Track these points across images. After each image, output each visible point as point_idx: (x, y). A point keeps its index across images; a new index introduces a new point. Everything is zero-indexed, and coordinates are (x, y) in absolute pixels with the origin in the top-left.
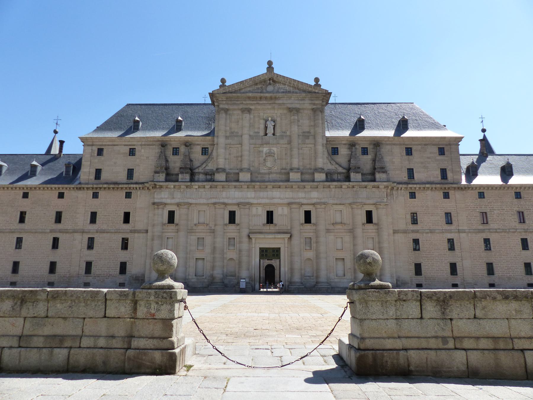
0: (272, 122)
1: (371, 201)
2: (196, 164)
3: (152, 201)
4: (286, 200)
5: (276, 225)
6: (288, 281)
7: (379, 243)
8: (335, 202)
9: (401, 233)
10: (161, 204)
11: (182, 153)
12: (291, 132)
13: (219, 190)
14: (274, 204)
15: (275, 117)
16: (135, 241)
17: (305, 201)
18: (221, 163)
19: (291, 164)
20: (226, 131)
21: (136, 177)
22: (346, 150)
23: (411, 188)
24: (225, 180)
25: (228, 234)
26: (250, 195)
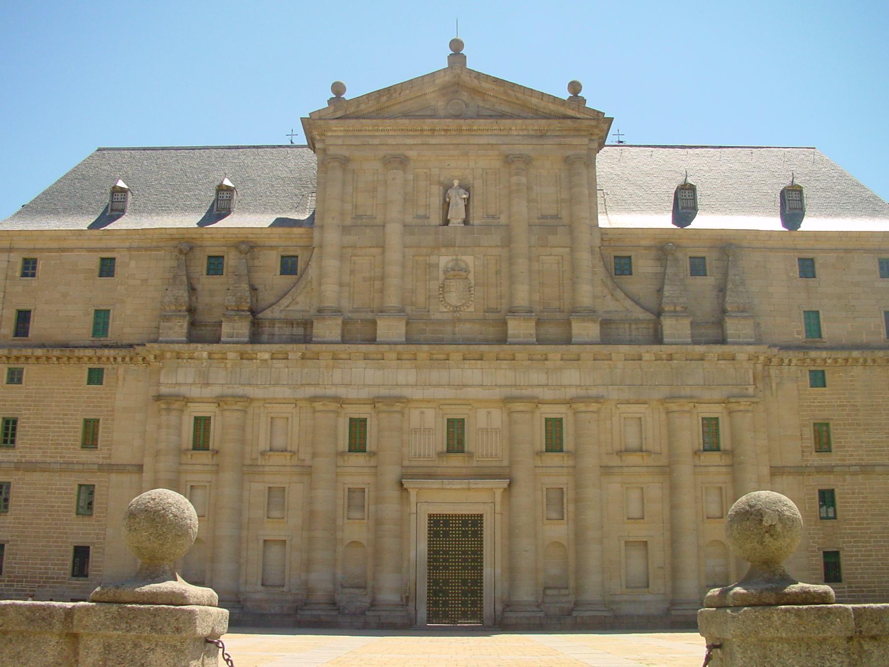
0: (462, 191)
2: (266, 296)
3: (153, 392)
4: (497, 390)
5: (471, 455)
9: (790, 473)
10: (177, 397)
13: (323, 363)
14: (466, 402)
15: (470, 177)
17: (548, 394)
18: (331, 294)
20: (342, 214)
21: (118, 328)
23: (814, 360)
24: (339, 339)
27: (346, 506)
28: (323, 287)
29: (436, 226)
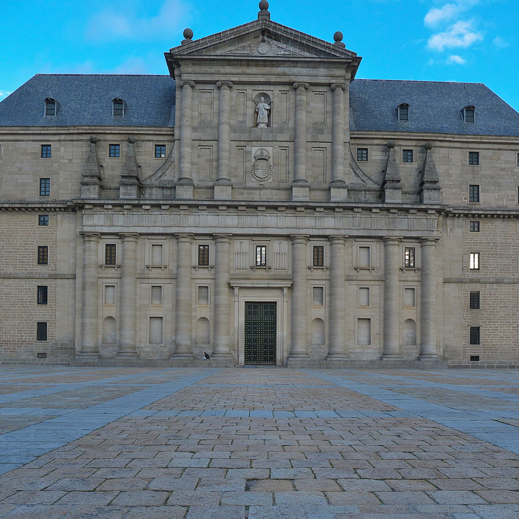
1: (414, 234)
2: (146, 173)
6: (287, 352)
7: (423, 296)
8: (361, 233)
11: (124, 154)
12: (295, 122)
15: (271, 96)
16: (59, 291)
19: (295, 173)
20: (192, 118)
22: (379, 153)
25: (198, 281)
26: (230, 222)
27: (197, 297)
28: (182, 165)
29: (250, 128)
